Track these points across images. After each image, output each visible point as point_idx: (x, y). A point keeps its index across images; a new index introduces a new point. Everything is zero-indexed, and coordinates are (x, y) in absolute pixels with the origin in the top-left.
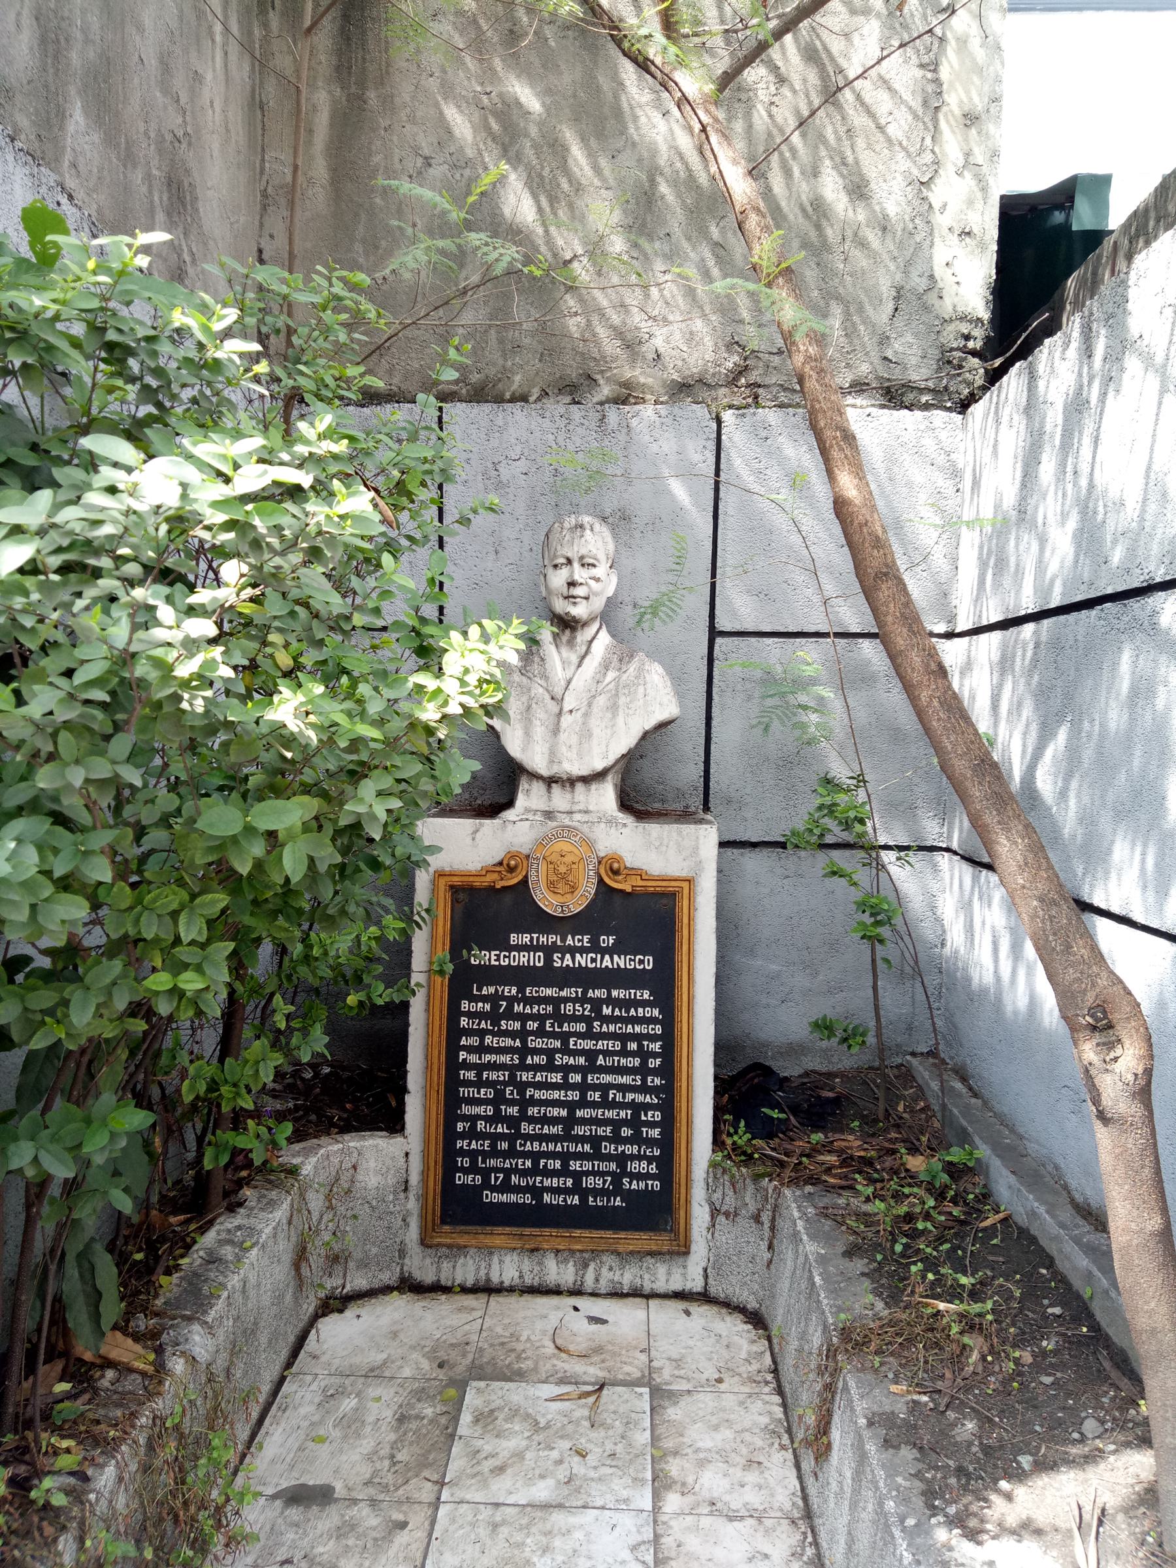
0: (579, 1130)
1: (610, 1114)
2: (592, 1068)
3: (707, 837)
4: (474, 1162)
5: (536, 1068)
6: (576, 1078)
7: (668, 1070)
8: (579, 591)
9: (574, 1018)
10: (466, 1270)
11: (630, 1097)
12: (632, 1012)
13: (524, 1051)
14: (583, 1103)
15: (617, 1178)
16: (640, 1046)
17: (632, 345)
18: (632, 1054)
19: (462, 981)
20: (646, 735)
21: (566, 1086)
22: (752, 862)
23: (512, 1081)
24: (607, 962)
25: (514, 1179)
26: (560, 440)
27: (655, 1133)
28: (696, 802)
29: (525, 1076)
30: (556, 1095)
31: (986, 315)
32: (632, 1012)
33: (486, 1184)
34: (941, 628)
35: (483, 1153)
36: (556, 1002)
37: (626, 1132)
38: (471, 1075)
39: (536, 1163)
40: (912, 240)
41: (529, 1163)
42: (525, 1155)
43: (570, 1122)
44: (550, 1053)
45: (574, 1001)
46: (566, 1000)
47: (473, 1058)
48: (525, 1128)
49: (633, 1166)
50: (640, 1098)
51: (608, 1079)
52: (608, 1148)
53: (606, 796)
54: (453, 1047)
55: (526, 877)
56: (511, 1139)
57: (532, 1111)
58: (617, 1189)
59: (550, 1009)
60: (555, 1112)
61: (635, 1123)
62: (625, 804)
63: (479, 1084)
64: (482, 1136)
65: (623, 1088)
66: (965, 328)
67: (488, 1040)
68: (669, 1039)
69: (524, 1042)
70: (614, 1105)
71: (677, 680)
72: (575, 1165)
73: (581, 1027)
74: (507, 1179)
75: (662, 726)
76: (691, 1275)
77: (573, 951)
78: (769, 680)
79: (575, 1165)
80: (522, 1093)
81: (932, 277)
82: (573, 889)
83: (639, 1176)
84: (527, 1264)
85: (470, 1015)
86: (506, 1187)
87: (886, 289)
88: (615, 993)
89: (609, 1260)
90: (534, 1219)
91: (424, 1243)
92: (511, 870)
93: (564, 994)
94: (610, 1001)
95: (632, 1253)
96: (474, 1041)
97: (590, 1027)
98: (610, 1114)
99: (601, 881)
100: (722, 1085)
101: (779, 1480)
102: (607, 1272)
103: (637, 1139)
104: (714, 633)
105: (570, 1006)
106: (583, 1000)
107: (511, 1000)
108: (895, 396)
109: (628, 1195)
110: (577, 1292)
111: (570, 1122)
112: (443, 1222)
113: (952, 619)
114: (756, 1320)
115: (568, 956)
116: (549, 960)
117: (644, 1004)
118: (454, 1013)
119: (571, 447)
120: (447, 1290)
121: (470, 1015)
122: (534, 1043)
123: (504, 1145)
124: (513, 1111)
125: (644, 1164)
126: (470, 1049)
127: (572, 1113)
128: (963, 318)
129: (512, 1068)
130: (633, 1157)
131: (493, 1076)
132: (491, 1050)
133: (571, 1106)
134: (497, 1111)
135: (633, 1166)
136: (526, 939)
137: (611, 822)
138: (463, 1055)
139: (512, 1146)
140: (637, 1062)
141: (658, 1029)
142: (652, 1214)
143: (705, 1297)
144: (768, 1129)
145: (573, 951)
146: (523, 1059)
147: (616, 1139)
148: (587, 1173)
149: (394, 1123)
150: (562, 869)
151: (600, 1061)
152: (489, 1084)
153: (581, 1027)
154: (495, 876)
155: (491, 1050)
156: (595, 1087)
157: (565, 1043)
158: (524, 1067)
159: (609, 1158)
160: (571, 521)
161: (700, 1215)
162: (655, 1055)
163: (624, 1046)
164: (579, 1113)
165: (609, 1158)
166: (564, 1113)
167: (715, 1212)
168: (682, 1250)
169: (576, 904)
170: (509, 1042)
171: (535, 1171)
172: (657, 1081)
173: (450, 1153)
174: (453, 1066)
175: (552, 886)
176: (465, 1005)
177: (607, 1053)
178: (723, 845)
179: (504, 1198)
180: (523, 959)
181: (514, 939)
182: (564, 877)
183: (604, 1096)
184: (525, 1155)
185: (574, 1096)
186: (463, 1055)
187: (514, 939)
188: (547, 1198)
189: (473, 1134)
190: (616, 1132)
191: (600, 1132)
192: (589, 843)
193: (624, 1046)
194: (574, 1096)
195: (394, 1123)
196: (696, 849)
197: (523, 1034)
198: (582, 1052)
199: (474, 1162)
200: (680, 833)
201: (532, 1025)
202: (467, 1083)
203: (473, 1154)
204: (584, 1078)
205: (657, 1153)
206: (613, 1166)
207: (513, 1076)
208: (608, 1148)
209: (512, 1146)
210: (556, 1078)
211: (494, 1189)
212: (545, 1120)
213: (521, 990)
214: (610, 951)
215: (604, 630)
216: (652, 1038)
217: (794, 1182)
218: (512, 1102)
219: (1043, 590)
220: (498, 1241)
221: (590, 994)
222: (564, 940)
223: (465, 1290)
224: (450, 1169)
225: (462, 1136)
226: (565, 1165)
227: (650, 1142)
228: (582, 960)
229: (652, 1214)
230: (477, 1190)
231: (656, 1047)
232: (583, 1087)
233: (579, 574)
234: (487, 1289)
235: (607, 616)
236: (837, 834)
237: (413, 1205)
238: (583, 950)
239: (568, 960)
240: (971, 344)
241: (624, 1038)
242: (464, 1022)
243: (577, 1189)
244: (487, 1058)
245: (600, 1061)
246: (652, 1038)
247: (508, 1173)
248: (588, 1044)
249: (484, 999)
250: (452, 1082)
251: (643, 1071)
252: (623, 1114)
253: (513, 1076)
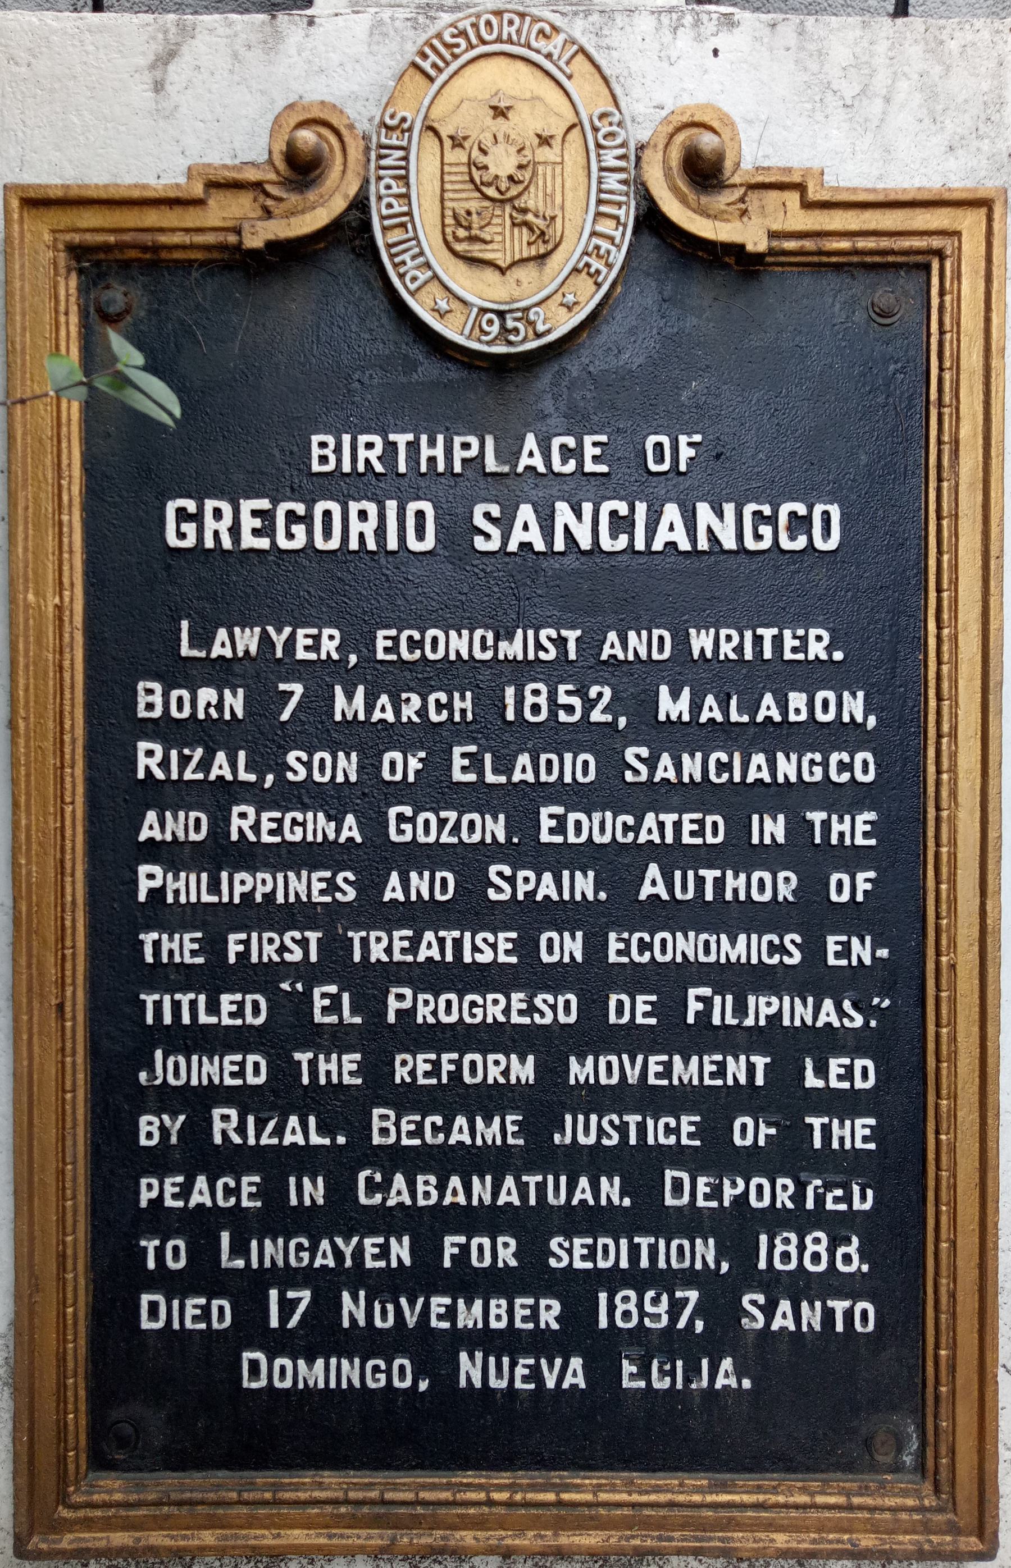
0: (580, 1131)
1: (687, 1071)
2: (622, 907)
4: (203, 1252)
5: (419, 915)
9: (554, 737)
11: (762, 1007)
12: (768, 708)
13: (374, 858)
14: (594, 1035)
15: (720, 1297)
16: (799, 828)
18: (771, 857)
21: (530, 975)
23: (335, 962)
24: (672, 529)
25: (352, 1308)
27: (857, 1133)
30: (493, 1008)
32: (768, 708)
33: (250, 1327)
35: (236, 1218)
36: (485, 678)
37: (749, 1131)
38: (183, 947)
39: (426, 1249)
41: (401, 1251)
42: (388, 1221)
43: (545, 1103)
44: (470, 862)
45: (554, 672)
46: (522, 671)
47: (189, 887)
49: (779, 1251)
50: (798, 1012)
51: (686, 945)
52: (685, 1189)
54: (112, 851)
55: (360, 204)
56: (338, 1167)
57: (411, 1067)
58: (722, 1332)
59: (464, 704)
60: (493, 1068)
61: (783, 1098)
63: (214, 976)
64: (233, 1160)
65: (740, 980)
67: (241, 820)
69: (374, 824)
70: (705, 1037)
72: (569, 1253)
73: (579, 767)
74: (326, 1305)
79: (569, 1253)
80: (370, 1004)
83: (800, 1286)
85: (169, 731)
88: (701, 642)
93: (512, 649)
94: (684, 669)
96: (186, 825)
97: (612, 764)
98: (687, 1071)
99: (651, 220)
103: (790, 1155)
105: (536, 692)
106: (585, 669)
107: (322, 676)
109: (762, 1352)
111: (545, 1103)
112: (100, 1461)
115: (526, 512)
117: (810, 675)
118: (112, 724)
121: (169, 731)
122: (409, 826)
123: (314, 1191)
124: (343, 1068)
125: (817, 1242)
126: (170, 855)
127: (551, 1070)
129: (327, 918)
130: (775, 1220)
131: (265, 947)
132: (249, 856)
133: (550, 1046)
134: (283, 1070)
135: (779, 1251)
136: (369, 450)
138: (149, 877)
139: (341, 1191)
140: (786, 885)
141: (865, 767)
145: (545, 490)
146: (370, 886)
147: (716, 1155)
148: (613, 1280)
150: (502, 163)
151: (652, 884)
153: (579, 767)
154: (238, 207)
155: (249, 856)
156: (635, 979)
157: (523, 822)
158: (374, 912)
159: (690, 1223)
162: (852, 858)
163: (738, 828)
164: (579, 1071)
165: (690, 1223)
166: (525, 1071)
170: (318, 826)
171: (424, 1277)
172: (862, 951)
173: (116, 1226)
176: (150, 698)
177: (673, 856)
179: (315, 1374)
180: (360, 524)
181: (324, 451)
183: (670, 1007)
184: (388, 1221)
186: (149, 877)
187: (324, 451)
188: (470, 1368)
189: (197, 1155)
190: (715, 1132)
191: (657, 1134)
193: (738, 828)
197: (369, 797)
198: (586, 857)
199: (203, 1252)
200: (935, 48)
201: (402, 765)
204: (595, 947)
205: (863, 1203)
206: (706, 1251)
207: (335, 948)
208: (685, 1189)
209: (341, 1191)
210: (493, 948)
211: (278, 1344)
212: (456, 1098)
213: (356, 638)
216: (844, 798)
218: (337, 1040)
221: (611, 647)
222: (510, 453)
224: (117, 1279)
225: (158, 1161)
226: (532, 1252)
228: (577, 525)
230: (220, 1350)
231: (857, 828)
232: (592, 979)
238: (582, 488)
239: (526, 530)
241: (739, 801)
242: (149, 758)
243: (578, 1333)
244: (241, 883)
245: (652, 884)
246: (844, 798)
247: (327, 1285)
248: (603, 828)
249: (222, 673)
251: (810, 913)
252: (736, 1069)
253: (335, 948)
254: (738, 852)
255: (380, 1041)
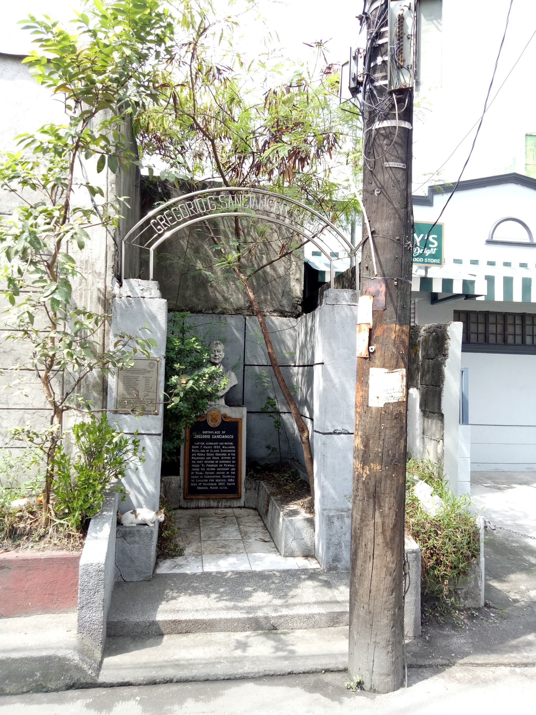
0: (218, 473)
2: (220, 460)
3: (244, 410)
5: (208, 460)
6: (217, 462)
7: (237, 459)
9: (217, 449)
10: (193, 504)
13: (206, 456)
14: (218, 467)
15: (226, 483)
17: (226, 299)
19: (192, 441)
21: (215, 464)
22: (254, 417)
27: (234, 473)
28: (241, 403)
29: (206, 462)
31: (302, 297)
33: (198, 485)
34: (293, 365)
36: (213, 446)
37: (228, 473)
38: (194, 462)
40: (285, 280)
43: (216, 471)
44: (211, 457)
48: (206, 473)
49: (229, 480)
52: (224, 476)
53: (222, 402)
54: (190, 456)
56: (203, 475)
57: (208, 469)
60: (213, 469)
61: (230, 471)
62: (226, 403)
63: (196, 464)
64: (197, 475)
65: (227, 464)
66: (297, 299)
68: (237, 453)
71: (237, 375)
72: (217, 481)
75: (234, 386)
76: (242, 503)
77: (216, 435)
78: (256, 375)
79: (217, 481)
82: (216, 421)
83: (230, 482)
84: (207, 502)
86: (202, 486)
87: (280, 291)
89: (224, 501)
90: (208, 493)
91: (185, 499)
94: (224, 445)
95: (229, 499)
96: (195, 455)
101: (261, 524)
102: (224, 503)
103: (230, 474)
104: (245, 365)
106: (218, 445)
107: (203, 446)
108: (283, 314)
109: (228, 486)
110: (217, 507)
111: (216, 471)
113: (295, 363)
114: (255, 509)
116: (211, 437)
118: (191, 449)
120: (190, 509)
122: (208, 455)
124: (204, 469)
129: (203, 460)
132: (199, 456)
133: (216, 468)
135: (229, 480)
137: (224, 407)
142: (233, 491)
143: (244, 507)
144: (257, 471)
145: (216, 435)
147: (226, 475)
149: (178, 474)
152: (198, 464)
155: (199, 456)
158: (206, 460)
159: (224, 479)
160: (215, 342)
161: (243, 490)
165: (224, 479)
167: (246, 490)
168: (239, 498)
169: (217, 425)
174: (190, 460)
175: (212, 421)
177: (224, 456)
178: (248, 412)
180: (205, 437)
181: (203, 432)
182: (214, 419)
185: (217, 466)
187: (203, 432)
189: (195, 475)
192: (219, 412)
194: (217, 466)
195: (178, 474)
196: (242, 413)
197: (206, 453)
201: (207, 451)
202: (194, 464)
203: (195, 479)
208: (224, 476)
210: (213, 462)
212: (211, 471)
214: (224, 434)
216: (233, 453)
217: (263, 480)
219: (308, 362)
220: (200, 497)
223: (193, 508)
224: (190, 482)
227: (233, 475)
228: (218, 437)
229: (233, 491)
230: (196, 487)
231: (234, 455)
232: (219, 464)
233: (217, 354)
234: (198, 508)
235: (222, 363)
236: (270, 409)
237: (182, 491)
238: (218, 434)
241: (227, 453)
243: (217, 485)
246: (233, 453)
248: (219, 455)
250: (190, 464)
251: (231, 460)
254: (227, 456)
255: (206, 468)
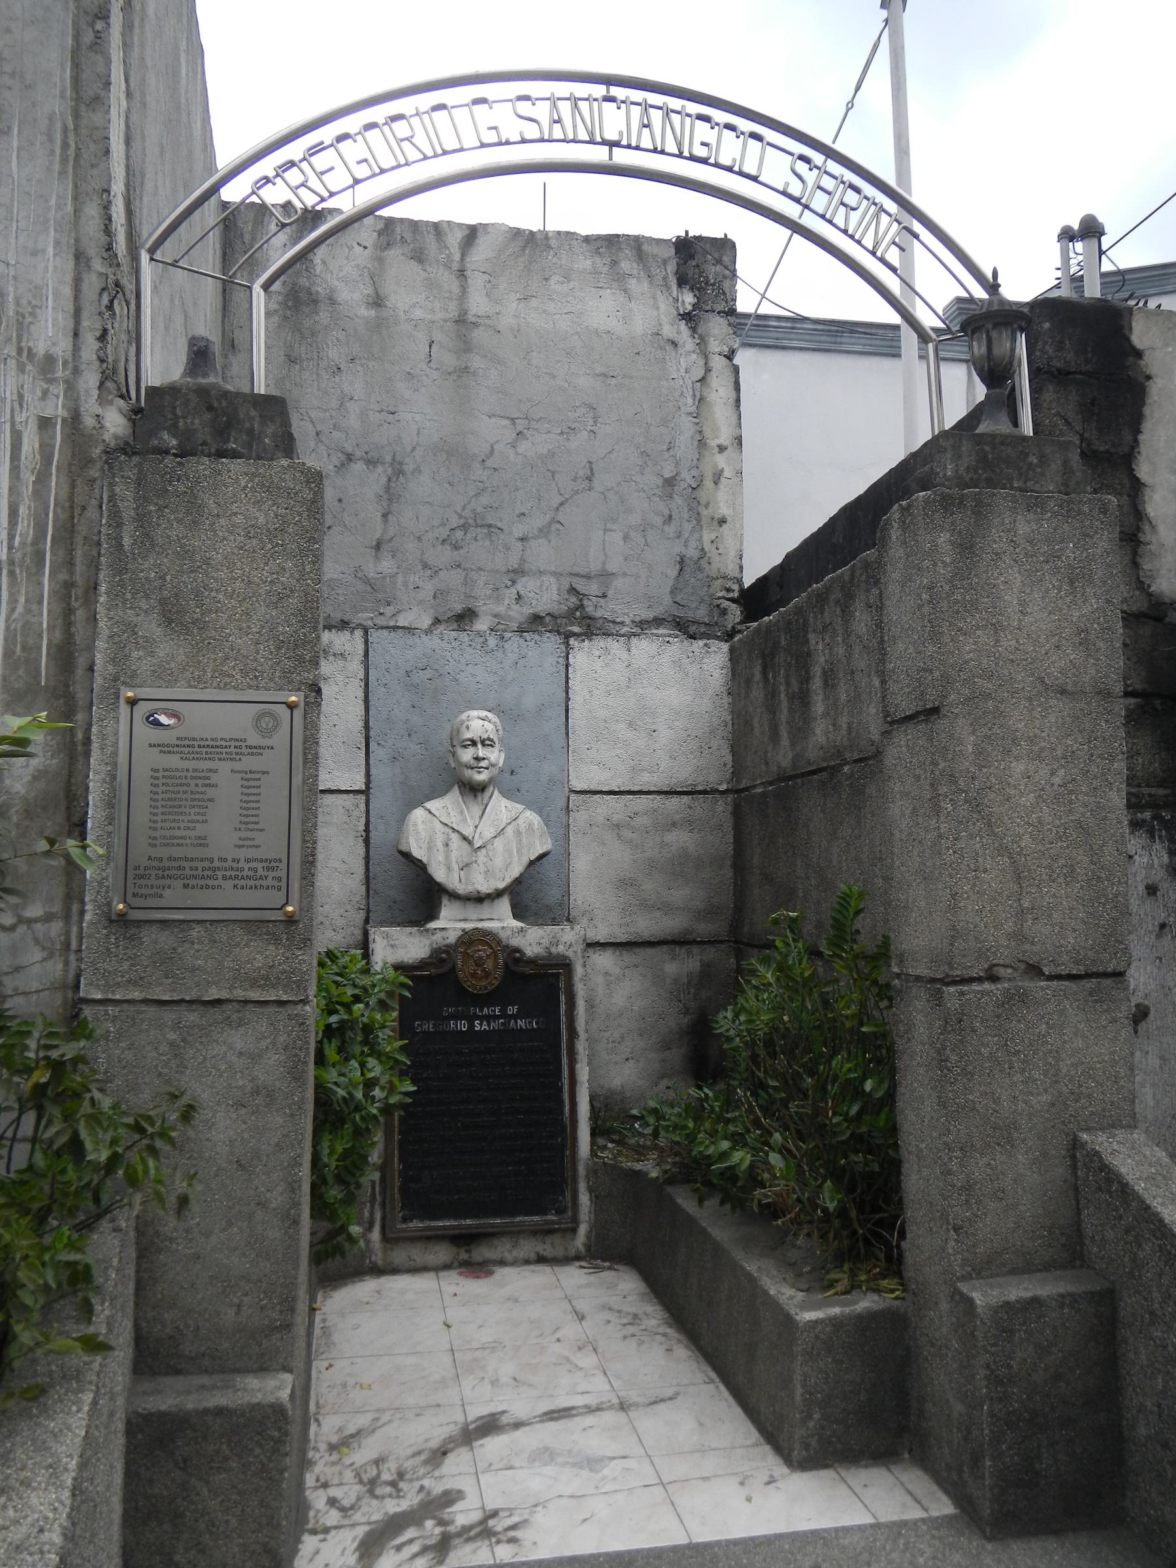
8: (484, 764)
20: (531, 863)
26: (455, 656)
53: (504, 906)
81: (703, 549)
92: (442, 961)
100: (594, 1115)
119: (463, 661)
128: (724, 577)
214: (515, 1017)
215: (496, 792)
222: (481, 1011)
240: (731, 595)
